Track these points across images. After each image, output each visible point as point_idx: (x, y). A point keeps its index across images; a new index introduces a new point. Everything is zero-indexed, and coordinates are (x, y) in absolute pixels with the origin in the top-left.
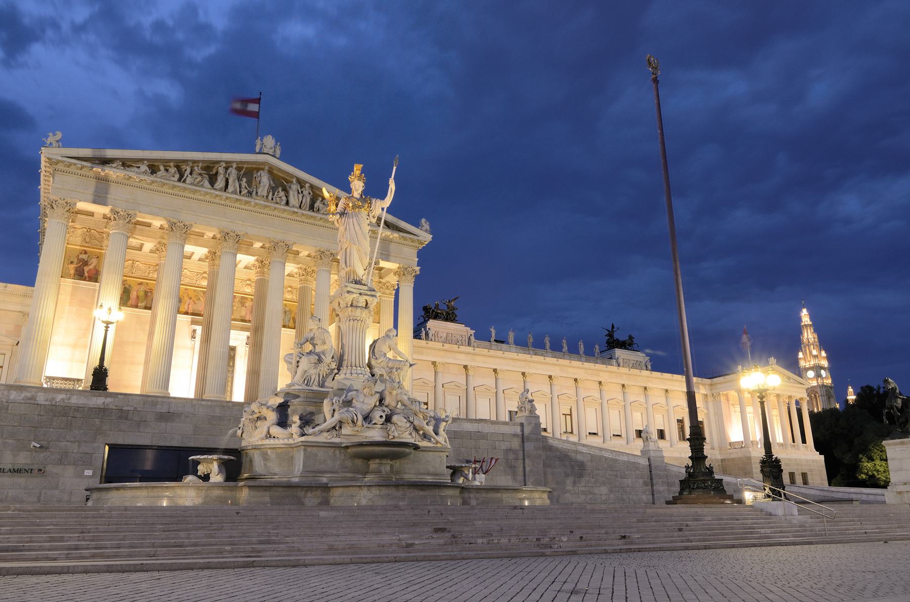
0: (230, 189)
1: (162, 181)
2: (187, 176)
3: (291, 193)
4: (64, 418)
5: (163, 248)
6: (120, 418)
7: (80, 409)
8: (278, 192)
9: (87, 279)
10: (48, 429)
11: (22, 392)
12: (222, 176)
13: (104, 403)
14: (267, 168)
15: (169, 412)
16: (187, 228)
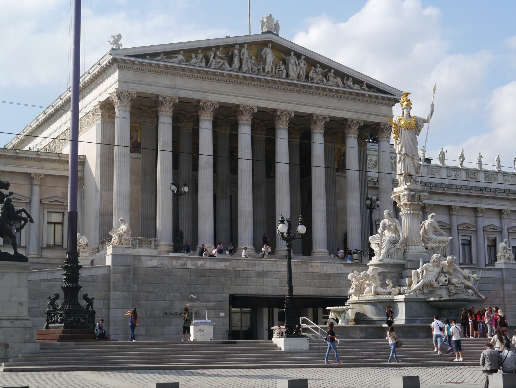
0: (245, 68)
1: (196, 68)
2: (212, 61)
3: (290, 66)
4: (204, 277)
5: (184, 118)
6: (235, 276)
7: (212, 270)
8: (280, 66)
10: (196, 285)
11: (179, 261)
12: (237, 57)
13: (225, 266)
14: (270, 44)
15: (264, 271)
16: (214, 106)
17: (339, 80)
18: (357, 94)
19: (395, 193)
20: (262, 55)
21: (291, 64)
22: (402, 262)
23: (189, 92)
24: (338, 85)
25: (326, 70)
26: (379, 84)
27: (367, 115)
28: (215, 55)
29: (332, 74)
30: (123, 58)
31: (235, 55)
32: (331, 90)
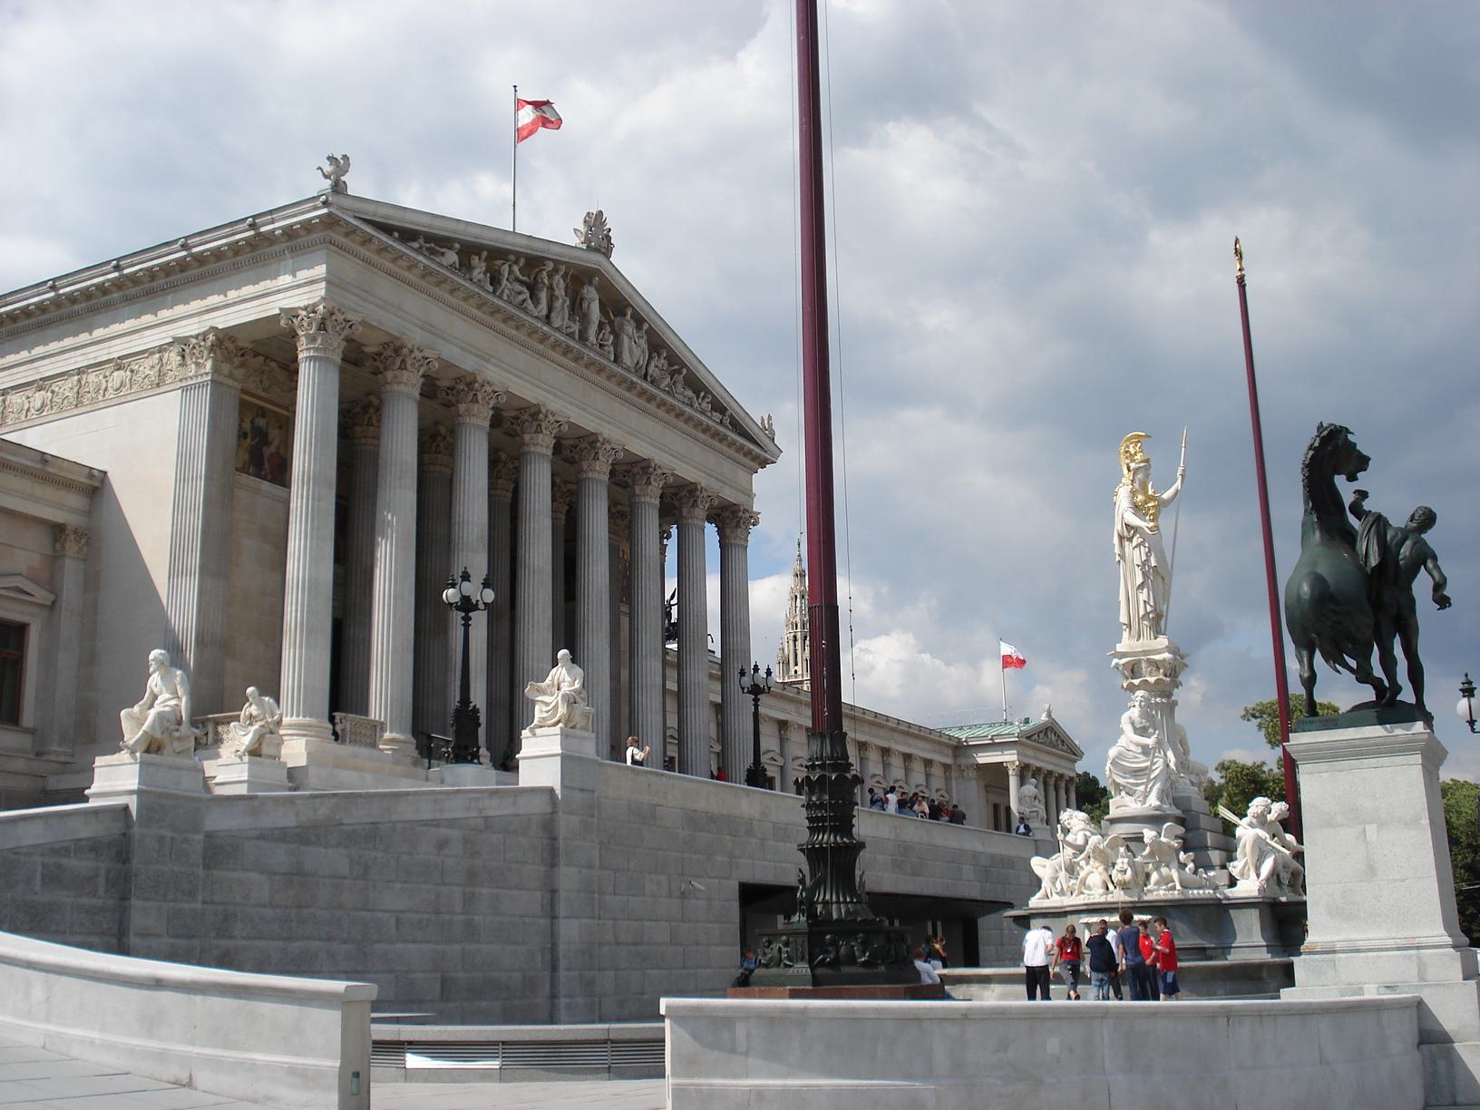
0: (557, 322)
3: (626, 340)
9: (269, 477)
17: (690, 393)
18: (715, 435)
19: (1123, 655)
20: (582, 299)
21: (627, 335)
22: (1178, 812)
23: (455, 349)
24: (691, 406)
25: (676, 367)
26: (747, 419)
27: (720, 484)
28: (510, 272)
29: (681, 377)
30: (352, 221)
31: (541, 285)
32: (679, 415)
